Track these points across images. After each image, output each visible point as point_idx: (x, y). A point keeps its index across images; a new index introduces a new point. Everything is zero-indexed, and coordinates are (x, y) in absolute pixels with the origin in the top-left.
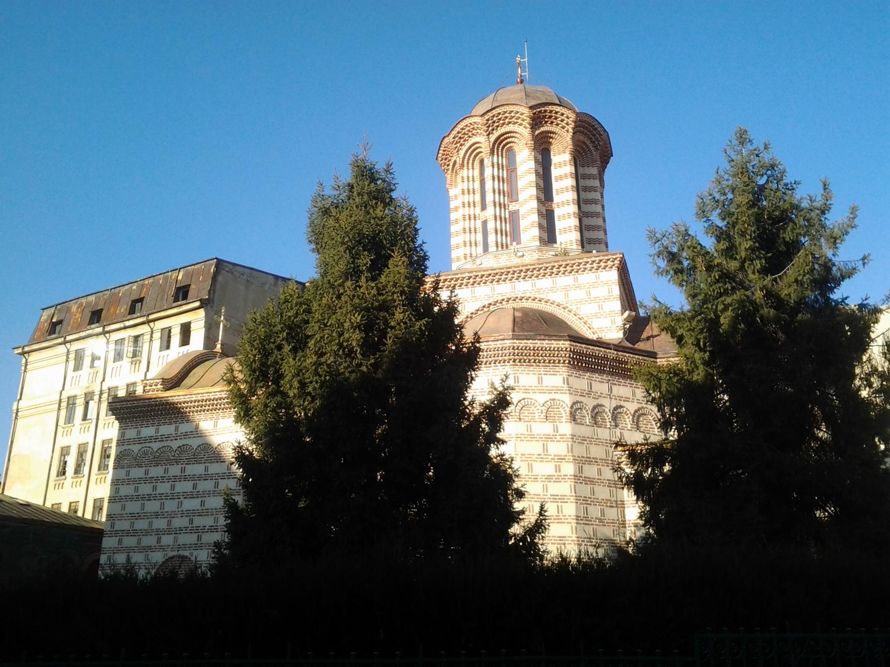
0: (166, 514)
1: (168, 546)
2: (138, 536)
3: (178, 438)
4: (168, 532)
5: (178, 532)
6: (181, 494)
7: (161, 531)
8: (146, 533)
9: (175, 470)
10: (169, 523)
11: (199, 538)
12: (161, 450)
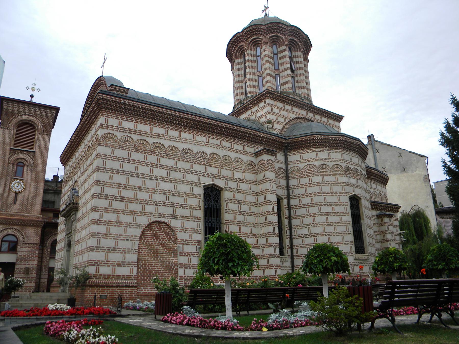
0: (147, 189)
2: (126, 202)
3: (153, 136)
4: (151, 203)
5: (158, 204)
6: (159, 177)
7: (145, 202)
8: (133, 201)
9: (152, 159)
10: (151, 197)
11: (174, 211)
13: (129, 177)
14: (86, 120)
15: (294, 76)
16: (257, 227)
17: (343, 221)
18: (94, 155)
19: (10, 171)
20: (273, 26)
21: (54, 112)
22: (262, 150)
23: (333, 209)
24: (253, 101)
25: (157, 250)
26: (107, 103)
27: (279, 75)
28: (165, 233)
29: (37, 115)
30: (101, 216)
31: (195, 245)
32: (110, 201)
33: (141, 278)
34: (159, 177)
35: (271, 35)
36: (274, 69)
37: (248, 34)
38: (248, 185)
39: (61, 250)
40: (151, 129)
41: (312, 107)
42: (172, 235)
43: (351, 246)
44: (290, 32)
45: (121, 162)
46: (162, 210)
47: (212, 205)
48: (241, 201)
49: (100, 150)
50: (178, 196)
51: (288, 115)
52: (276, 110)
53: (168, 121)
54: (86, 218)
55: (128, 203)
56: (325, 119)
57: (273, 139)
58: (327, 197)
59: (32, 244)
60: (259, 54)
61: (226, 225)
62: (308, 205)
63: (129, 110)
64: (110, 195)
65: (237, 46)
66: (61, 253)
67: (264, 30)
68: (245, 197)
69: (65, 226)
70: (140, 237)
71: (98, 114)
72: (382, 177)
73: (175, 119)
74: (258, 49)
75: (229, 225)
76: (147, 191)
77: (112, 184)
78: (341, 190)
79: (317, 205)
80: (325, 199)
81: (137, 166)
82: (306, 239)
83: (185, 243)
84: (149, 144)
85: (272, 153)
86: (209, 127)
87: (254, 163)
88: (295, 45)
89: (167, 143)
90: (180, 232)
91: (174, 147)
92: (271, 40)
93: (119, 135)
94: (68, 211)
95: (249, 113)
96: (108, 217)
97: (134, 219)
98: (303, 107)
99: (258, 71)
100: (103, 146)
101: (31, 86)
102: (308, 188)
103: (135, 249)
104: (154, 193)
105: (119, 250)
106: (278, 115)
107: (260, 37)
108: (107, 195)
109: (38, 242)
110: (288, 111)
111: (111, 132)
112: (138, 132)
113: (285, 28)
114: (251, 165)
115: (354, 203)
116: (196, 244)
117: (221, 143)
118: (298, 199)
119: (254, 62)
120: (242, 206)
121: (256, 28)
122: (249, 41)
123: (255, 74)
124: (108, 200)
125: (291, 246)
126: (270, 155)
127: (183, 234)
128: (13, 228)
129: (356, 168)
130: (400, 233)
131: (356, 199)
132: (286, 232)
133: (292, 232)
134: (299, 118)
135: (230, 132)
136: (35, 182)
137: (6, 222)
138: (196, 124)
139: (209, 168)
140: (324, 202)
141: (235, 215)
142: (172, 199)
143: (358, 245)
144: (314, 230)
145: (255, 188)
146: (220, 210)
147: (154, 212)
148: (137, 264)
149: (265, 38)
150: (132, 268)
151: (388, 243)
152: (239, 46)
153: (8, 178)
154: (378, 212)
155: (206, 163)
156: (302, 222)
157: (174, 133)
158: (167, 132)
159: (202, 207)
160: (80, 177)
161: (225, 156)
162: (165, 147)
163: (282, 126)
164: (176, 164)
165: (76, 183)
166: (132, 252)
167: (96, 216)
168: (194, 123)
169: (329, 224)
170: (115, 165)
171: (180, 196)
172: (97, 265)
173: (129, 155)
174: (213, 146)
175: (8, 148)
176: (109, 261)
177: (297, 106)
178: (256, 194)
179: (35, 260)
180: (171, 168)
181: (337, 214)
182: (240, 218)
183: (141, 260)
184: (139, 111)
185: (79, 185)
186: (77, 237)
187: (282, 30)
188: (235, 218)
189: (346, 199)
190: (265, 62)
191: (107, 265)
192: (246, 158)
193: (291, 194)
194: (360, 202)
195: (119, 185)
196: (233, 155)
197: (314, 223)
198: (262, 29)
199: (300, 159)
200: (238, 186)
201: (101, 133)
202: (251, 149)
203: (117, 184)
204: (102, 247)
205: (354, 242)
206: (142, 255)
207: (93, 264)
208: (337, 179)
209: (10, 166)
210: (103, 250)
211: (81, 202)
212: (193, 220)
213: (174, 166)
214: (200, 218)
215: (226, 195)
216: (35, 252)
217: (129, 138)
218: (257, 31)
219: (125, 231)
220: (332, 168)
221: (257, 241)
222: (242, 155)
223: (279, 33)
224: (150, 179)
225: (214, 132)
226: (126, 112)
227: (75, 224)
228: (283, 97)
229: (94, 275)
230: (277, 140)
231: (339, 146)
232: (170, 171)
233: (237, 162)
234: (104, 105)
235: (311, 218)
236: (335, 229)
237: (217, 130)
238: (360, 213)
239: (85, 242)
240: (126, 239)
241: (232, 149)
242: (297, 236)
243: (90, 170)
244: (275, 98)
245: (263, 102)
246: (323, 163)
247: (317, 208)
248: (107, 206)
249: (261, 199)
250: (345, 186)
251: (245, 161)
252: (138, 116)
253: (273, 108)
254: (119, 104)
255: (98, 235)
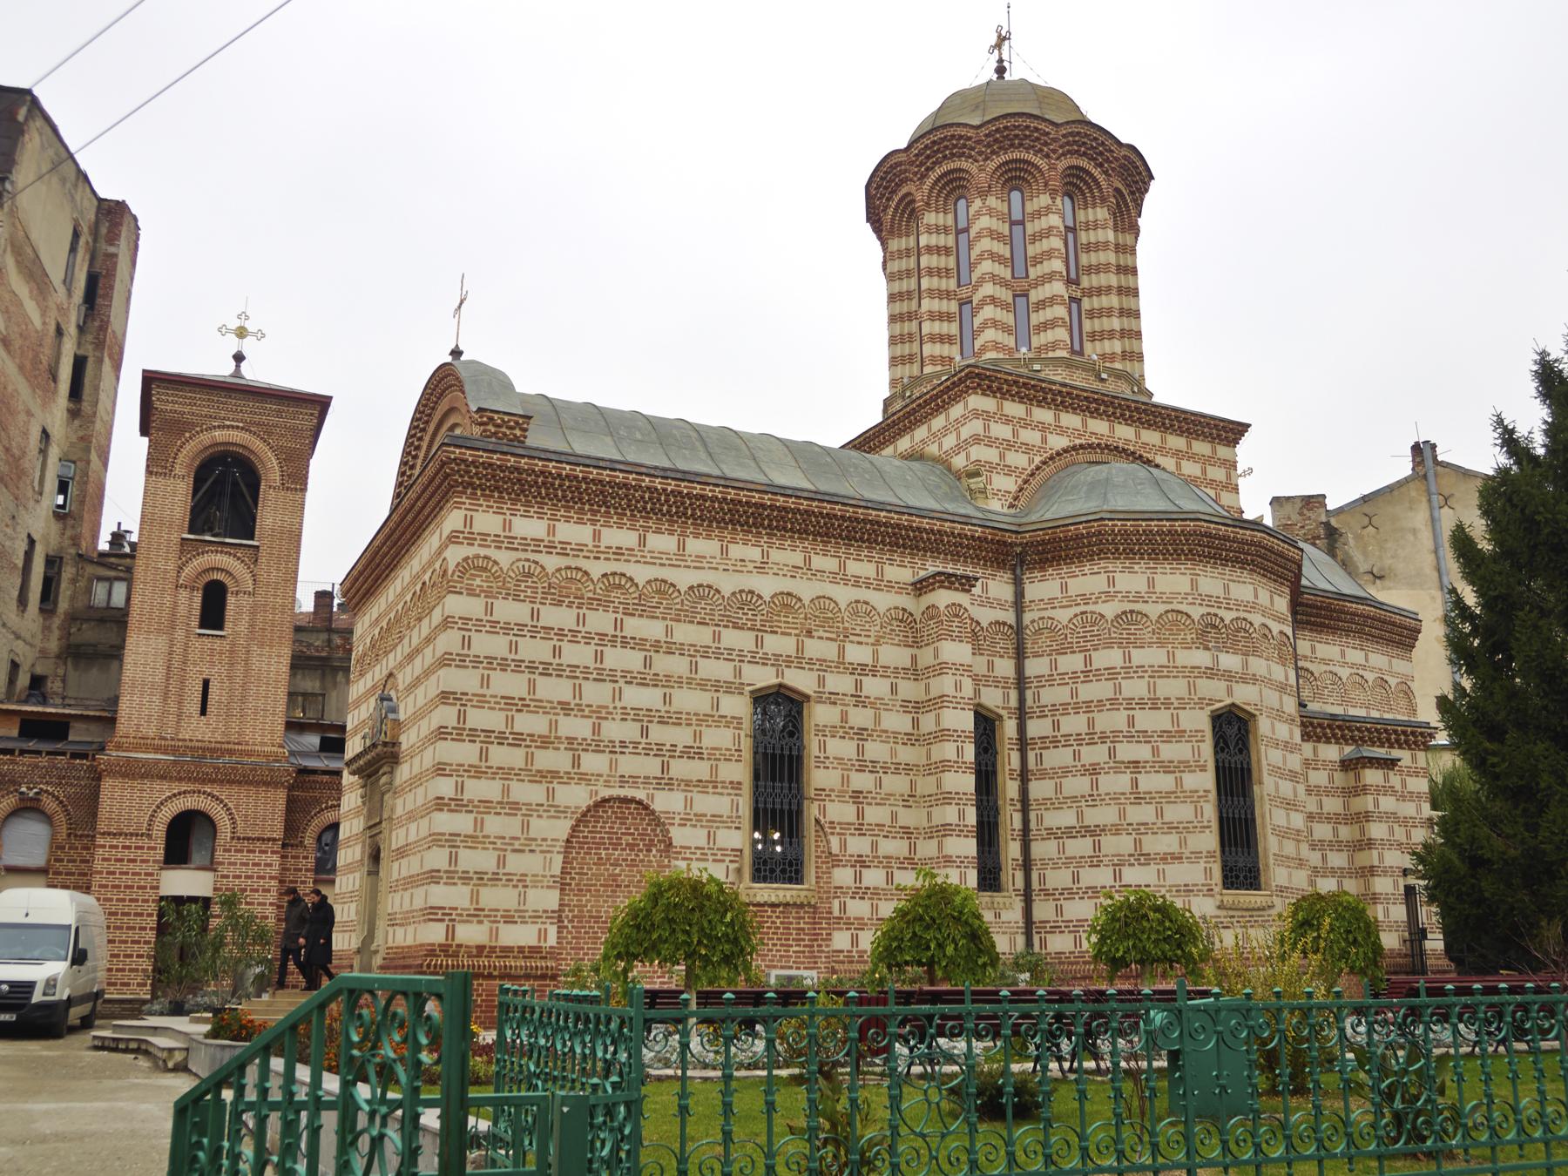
0: (587, 710)
1: (598, 775)
2: (527, 746)
3: (602, 556)
5: (618, 749)
6: (619, 674)
8: (545, 742)
9: (600, 621)
10: (596, 729)
11: (665, 767)
12: (580, 574)
13: (536, 676)
14: (413, 506)
15: (1079, 294)
16: (914, 805)
17: (1185, 788)
18: (437, 616)
19: (182, 610)
20: (1006, 128)
21: (312, 415)
22: (933, 576)
23: (1155, 751)
24: (934, 398)
25: (614, 877)
26: (468, 472)
27: (1027, 296)
28: (637, 829)
29: (258, 424)
30: (460, 788)
31: (723, 861)
32: (484, 745)
33: (568, 954)
34: (619, 674)
35: (1003, 158)
36: (1008, 276)
37: (928, 157)
38: (888, 681)
39: (350, 868)
40: (597, 536)
41: (1128, 407)
42: (657, 835)
43: (1208, 866)
44: (1068, 143)
45: (511, 637)
46: (629, 764)
47: (778, 746)
48: (866, 730)
49: (456, 605)
50: (673, 724)
51: (1044, 440)
52: (1001, 431)
53: (645, 508)
54: (421, 790)
55: (533, 749)
56: (1176, 442)
57: (973, 537)
58: (1138, 714)
59: (258, 839)
60: (962, 224)
61: (817, 803)
62: (1079, 739)
63: (532, 486)
64: (483, 731)
65: (894, 192)
66: (351, 877)
67: (979, 142)
68: (877, 720)
69: (364, 803)
70: (568, 841)
71: (444, 498)
72: (1394, 624)
73: (667, 501)
74: (962, 203)
75: (827, 803)
76: (586, 713)
77: (488, 699)
78: (1184, 693)
79: (1103, 738)
80: (1131, 721)
81: (558, 644)
82: (1069, 842)
83: (694, 857)
84: (592, 580)
85: (961, 584)
86: (768, 516)
87: (911, 615)
88: (1086, 183)
89: (642, 574)
90: (680, 825)
91: (665, 582)
92: (1002, 175)
93: (504, 558)
94: (370, 764)
95: (921, 433)
96: (479, 789)
97: (550, 794)
98: (1097, 410)
99: (959, 286)
100: (461, 593)
101: (234, 324)
102: (1079, 685)
103: (552, 876)
104: (606, 718)
105: (508, 880)
106: (1009, 445)
107: (964, 164)
108: (476, 730)
109: (278, 833)
110: (1043, 428)
111: (483, 552)
112: (559, 546)
113: (1048, 134)
114: (901, 621)
115: (1231, 732)
116: (727, 859)
117: (807, 561)
118: (1049, 721)
119: (947, 251)
120: (868, 745)
121: (953, 136)
122: (929, 182)
123: (947, 295)
124: (478, 745)
125: (1024, 861)
126: (956, 589)
127: (688, 830)
128: (199, 792)
129: (1245, 619)
130: (1430, 819)
131: (1240, 719)
132: (1011, 819)
133: (1029, 821)
134: (1082, 446)
135: (833, 525)
136: (262, 645)
137: (179, 773)
138: (729, 510)
139: (768, 638)
140: (1125, 728)
141: (846, 773)
142: (658, 733)
143: (1236, 862)
144: (1094, 817)
145: (909, 690)
146: (800, 758)
147: (605, 770)
148: (558, 917)
149: (980, 171)
150: (543, 927)
151: (1375, 853)
152: (900, 194)
153: (180, 634)
154: (1348, 749)
155: (758, 623)
156: (1058, 788)
157: (662, 542)
158: (642, 541)
159: (747, 755)
160: (401, 666)
161: (818, 598)
162: (637, 585)
163: (1020, 481)
164: (669, 631)
165: (391, 680)
166: (545, 884)
167: (445, 787)
168: (722, 509)
169: (1139, 798)
170: (494, 645)
171: (680, 724)
172: (450, 920)
173: (534, 614)
174: (781, 573)
175: (175, 537)
176: (483, 910)
177: (1074, 409)
178: (915, 708)
179: (269, 891)
180: (656, 647)
181: (1167, 768)
182: (862, 781)
183: (569, 905)
184: (560, 486)
185: (401, 687)
186: (397, 838)
187: (1038, 139)
188: (845, 780)
189: (1199, 721)
190: (981, 258)
191: (475, 919)
192: (883, 601)
193: (1029, 702)
194: (1251, 728)
195: (512, 704)
196: (844, 595)
197: (1095, 793)
198: (969, 138)
199: (1060, 596)
200: (858, 685)
201: (455, 555)
202: (902, 572)
203: (502, 697)
204: (463, 872)
205: (1218, 854)
206: (571, 890)
207: (439, 917)
208: (1171, 656)
209: (184, 594)
210: (466, 878)
211: (407, 740)
212: (719, 790)
213: (663, 639)
214: (739, 783)
215: (820, 715)
216: (271, 865)
217: (533, 566)
218: (955, 146)
219: (525, 826)
220: (1157, 622)
221: (913, 848)
222: (871, 591)
223: (1027, 149)
224: (595, 680)
225: (785, 529)
226: (523, 491)
227: (390, 802)
228: (1024, 384)
229: (440, 945)
230: (986, 539)
231: (1183, 550)
232: (652, 654)
233: (856, 613)
234: (461, 476)
235: (1087, 779)
236: (1160, 813)
237: (792, 523)
238: (1249, 763)
239: (419, 855)
240: (527, 848)
241: (841, 577)
242: (1044, 832)
243: (428, 656)
244: (999, 389)
245: (961, 405)
246: (1128, 607)
247: (1105, 747)
248: (475, 760)
249: (928, 723)
250: (1198, 681)
251: (882, 610)
252: (560, 501)
253: (992, 424)
254: (503, 471)
255: (452, 841)
